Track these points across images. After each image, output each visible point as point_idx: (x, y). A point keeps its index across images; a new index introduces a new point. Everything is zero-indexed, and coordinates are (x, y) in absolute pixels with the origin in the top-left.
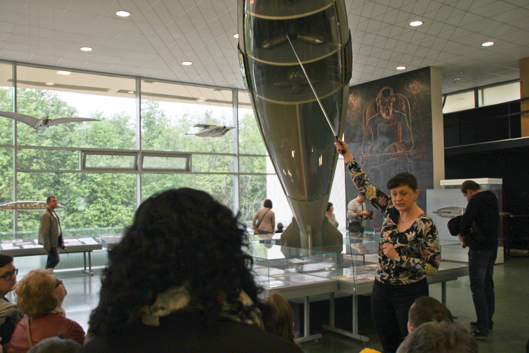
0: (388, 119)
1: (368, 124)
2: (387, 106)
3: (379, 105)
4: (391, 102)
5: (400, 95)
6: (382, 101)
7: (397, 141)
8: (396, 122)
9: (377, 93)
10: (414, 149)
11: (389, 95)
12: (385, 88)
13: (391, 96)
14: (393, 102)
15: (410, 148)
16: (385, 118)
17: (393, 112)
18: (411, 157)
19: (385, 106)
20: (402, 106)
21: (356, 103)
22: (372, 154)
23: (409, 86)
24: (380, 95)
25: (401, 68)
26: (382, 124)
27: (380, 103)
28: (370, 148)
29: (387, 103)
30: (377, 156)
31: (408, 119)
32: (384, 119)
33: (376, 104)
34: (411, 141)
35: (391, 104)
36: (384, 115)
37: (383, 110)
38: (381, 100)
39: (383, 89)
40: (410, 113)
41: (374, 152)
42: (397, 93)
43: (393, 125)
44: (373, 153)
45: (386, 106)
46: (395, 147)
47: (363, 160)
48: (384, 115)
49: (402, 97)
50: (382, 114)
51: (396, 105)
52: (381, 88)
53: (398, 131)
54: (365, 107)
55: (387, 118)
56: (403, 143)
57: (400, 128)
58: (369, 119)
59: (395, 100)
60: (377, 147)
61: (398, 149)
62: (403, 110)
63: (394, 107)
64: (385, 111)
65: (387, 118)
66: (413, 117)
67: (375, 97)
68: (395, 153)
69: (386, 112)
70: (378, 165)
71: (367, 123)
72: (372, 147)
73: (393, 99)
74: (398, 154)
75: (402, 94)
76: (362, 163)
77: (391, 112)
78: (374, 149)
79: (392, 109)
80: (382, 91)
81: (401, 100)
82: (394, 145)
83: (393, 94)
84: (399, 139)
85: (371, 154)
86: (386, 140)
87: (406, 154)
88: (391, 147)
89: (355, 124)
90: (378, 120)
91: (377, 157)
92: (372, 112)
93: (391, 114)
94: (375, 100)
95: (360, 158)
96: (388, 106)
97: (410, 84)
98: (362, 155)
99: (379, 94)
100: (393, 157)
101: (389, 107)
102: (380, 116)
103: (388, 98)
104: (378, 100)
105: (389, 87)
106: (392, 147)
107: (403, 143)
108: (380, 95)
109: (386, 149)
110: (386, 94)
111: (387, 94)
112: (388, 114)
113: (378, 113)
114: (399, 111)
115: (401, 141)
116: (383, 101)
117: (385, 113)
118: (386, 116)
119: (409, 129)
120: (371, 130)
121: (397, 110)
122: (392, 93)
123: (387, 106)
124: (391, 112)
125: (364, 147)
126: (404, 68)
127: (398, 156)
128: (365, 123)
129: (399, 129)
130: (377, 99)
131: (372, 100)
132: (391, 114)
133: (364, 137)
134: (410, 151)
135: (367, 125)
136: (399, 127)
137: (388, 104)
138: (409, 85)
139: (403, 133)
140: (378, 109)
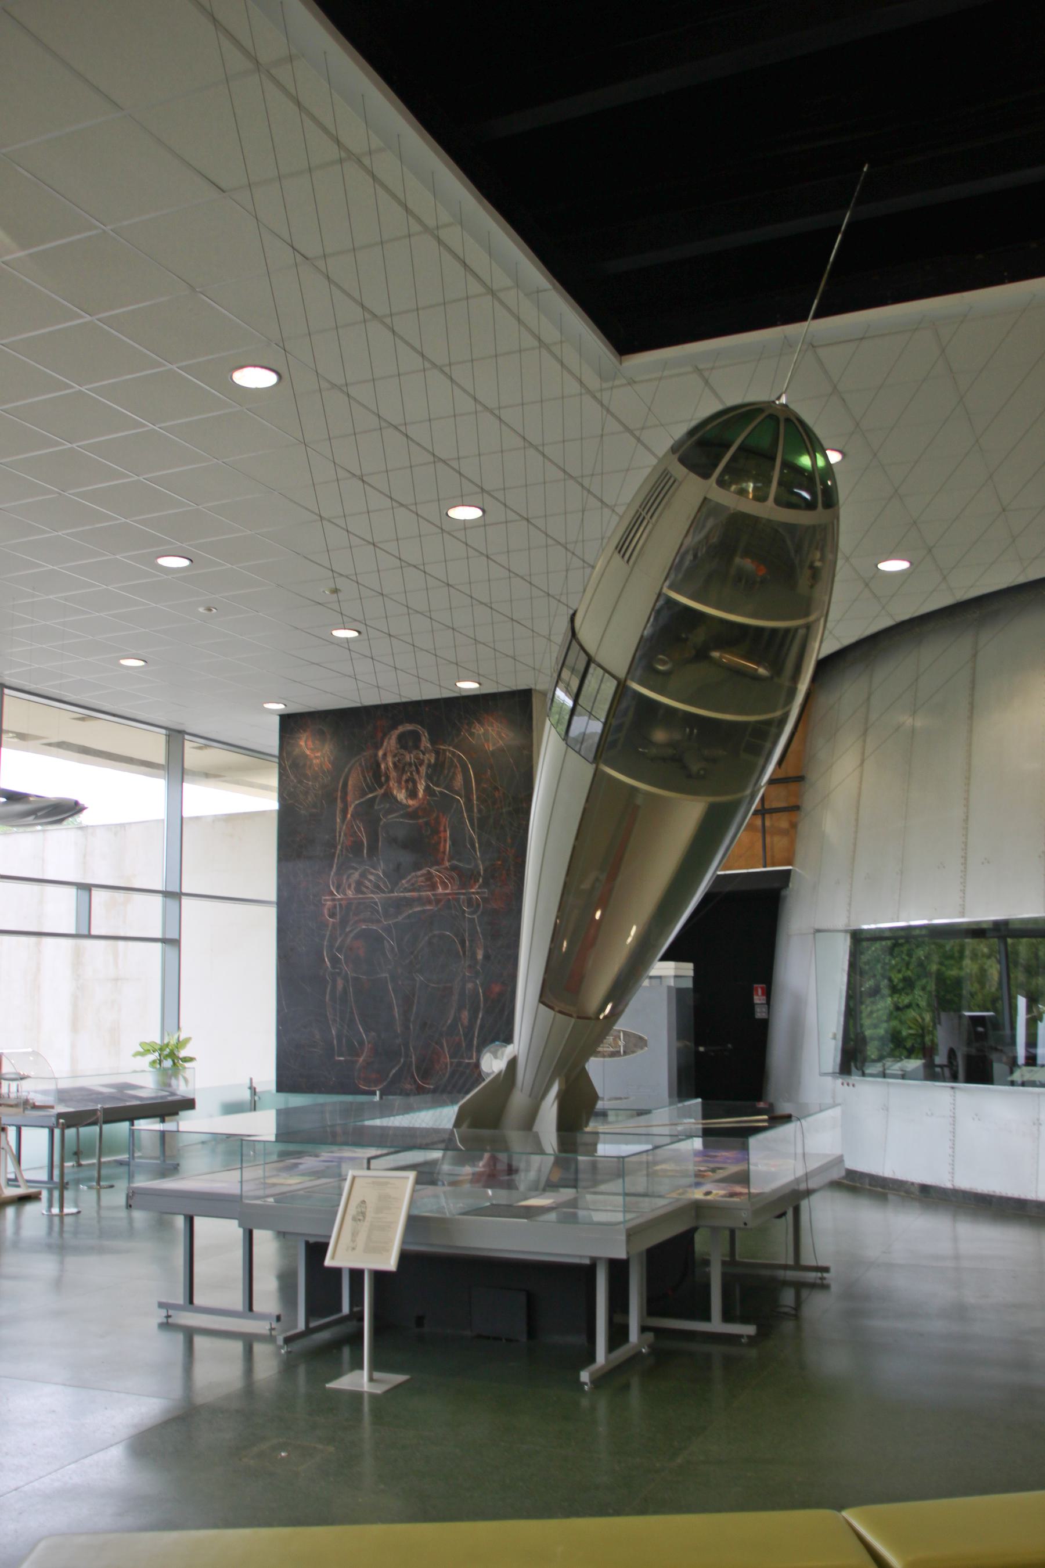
0: (413, 805)
1: (352, 816)
2: (411, 774)
3: (387, 768)
4: (421, 765)
5: (448, 749)
6: (397, 759)
7: (437, 863)
8: (435, 815)
9: (385, 735)
10: (486, 884)
11: (417, 747)
12: (409, 727)
13: (422, 748)
14: (429, 766)
15: (472, 882)
16: (404, 801)
17: (427, 789)
18: (475, 904)
19: (403, 771)
20: (453, 778)
21: (317, 757)
22: (363, 893)
23: (473, 731)
24: (391, 742)
25: (468, 686)
26: (396, 817)
27: (391, 765)
28: (356, 875)
29: (410, 764)
30: (376, 897)
31: (470, 810)
32: (401, 803)
33: (378, 765)
34: (477, 866)
35: (423, 770)
36: (401, 796)
37: (399, 782)
38: (395, 756)
39: (401, 729)
40: (475, 797)
41: (367, 888)
42: (442, 744)
43: (427, 823)
44: (364, 889)
45: (409, 774)
46: (429, 877)
47: (335, 907)
48: (401, 796)
49: (453, 753)
50: (395, 792)
51: (437, 771)
52: (394, 727)
53: (440, 838)
54: (347, 770)
55: (411, 802)
56: (454, 868)
57: (445, 831)
58: (357, 802)
59: (433, 761)
60: (378, 875)
61: (439, 885)
62: (456, 788)
63: (429, 777)
64: (403, 783)
65: (411, 802)
66: (482, 807)
67: (377, 746)
68: (429, 893)
69: (407, 789)
70: (379, 921)
71: (351, 810)
72: (363, 875)
73: (427, 755)
74: (439, 897)
75: (454, 748)
76: (332, 915)
77: (421, 788)
78: (370, 881)
79: (426, 782)
80: (395, 734)
81: (452, 761)
82: (429, 873)
83: (429, 745)
84: (443, 860)
85: (358, 890)
86: (406, 858)
87: (462, 897)
88: (420, 876)
89: (314, 810)
90: (382, 806)
91: (377, 900)
92: (367, 785)
93: (421, 794)
94: (376, 755)
95: (326, 900)
96: (414, 773)
97: (477, 724)
98: (332, 894)
99: (390, 739)
100: (424, 904)
101: (416, 777)
102: (388, 796)
103: (415, 752)
104: (385, 755)
105: (420, 727)
106: (421, 879)
107: (454, 868)
108: (391, 742)
109: (404, 882)
110: (408, 742)
111: (410, 744)
112: (412, 794)
113: (385, 787)
114: (445, 788)
115: (447, 864)
116: (399, 761)
117: (404, 791)
118: (406, 799)
119: (471, 835)
120: (361, 832)
121: (437, 787)
122: (425, 742)
123: (411, 774)
124: (421, 788)
125: (339, 873)
126: (475, 685)
127: (438, 901)
128: (345, 811)
129: (442, 835)
130: (380, 753)
131: (367, 754)
132: (421, 794)
133: (339, 847)
134: (473, 890)
135: (349, 816)
136: (442, 828)
137: (414, 768)
138: (475, 728)
139: (454, 842)
140: (383, 779)
